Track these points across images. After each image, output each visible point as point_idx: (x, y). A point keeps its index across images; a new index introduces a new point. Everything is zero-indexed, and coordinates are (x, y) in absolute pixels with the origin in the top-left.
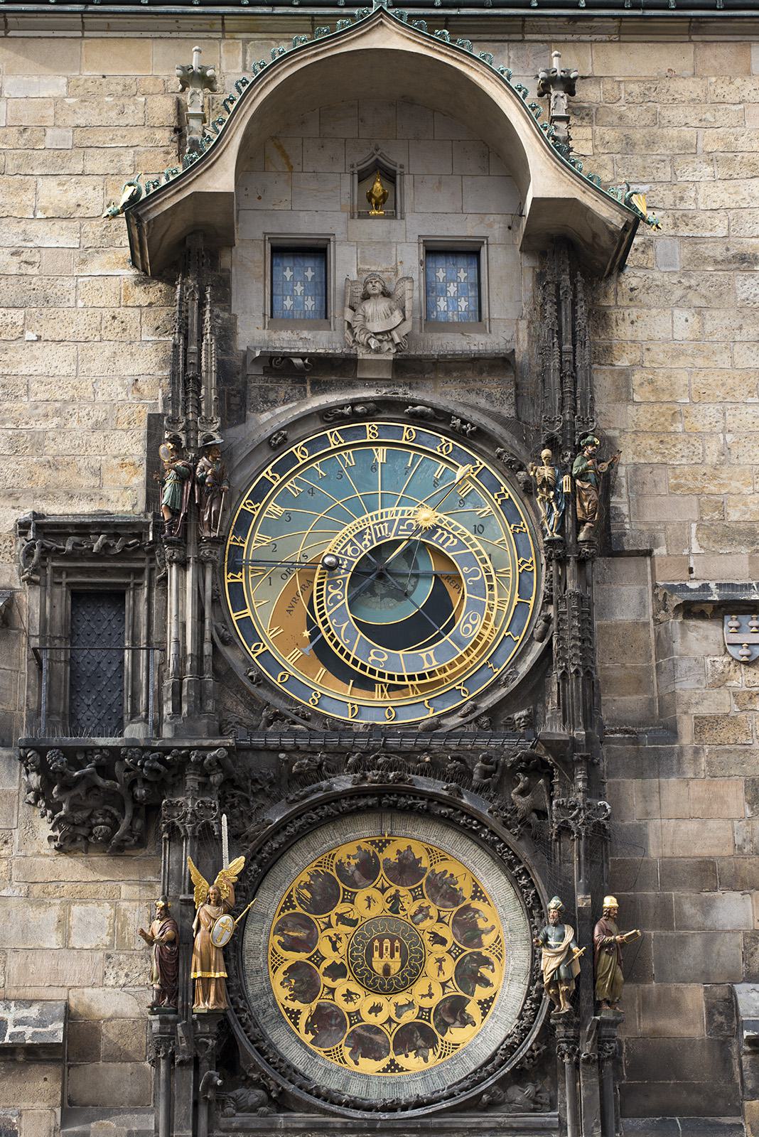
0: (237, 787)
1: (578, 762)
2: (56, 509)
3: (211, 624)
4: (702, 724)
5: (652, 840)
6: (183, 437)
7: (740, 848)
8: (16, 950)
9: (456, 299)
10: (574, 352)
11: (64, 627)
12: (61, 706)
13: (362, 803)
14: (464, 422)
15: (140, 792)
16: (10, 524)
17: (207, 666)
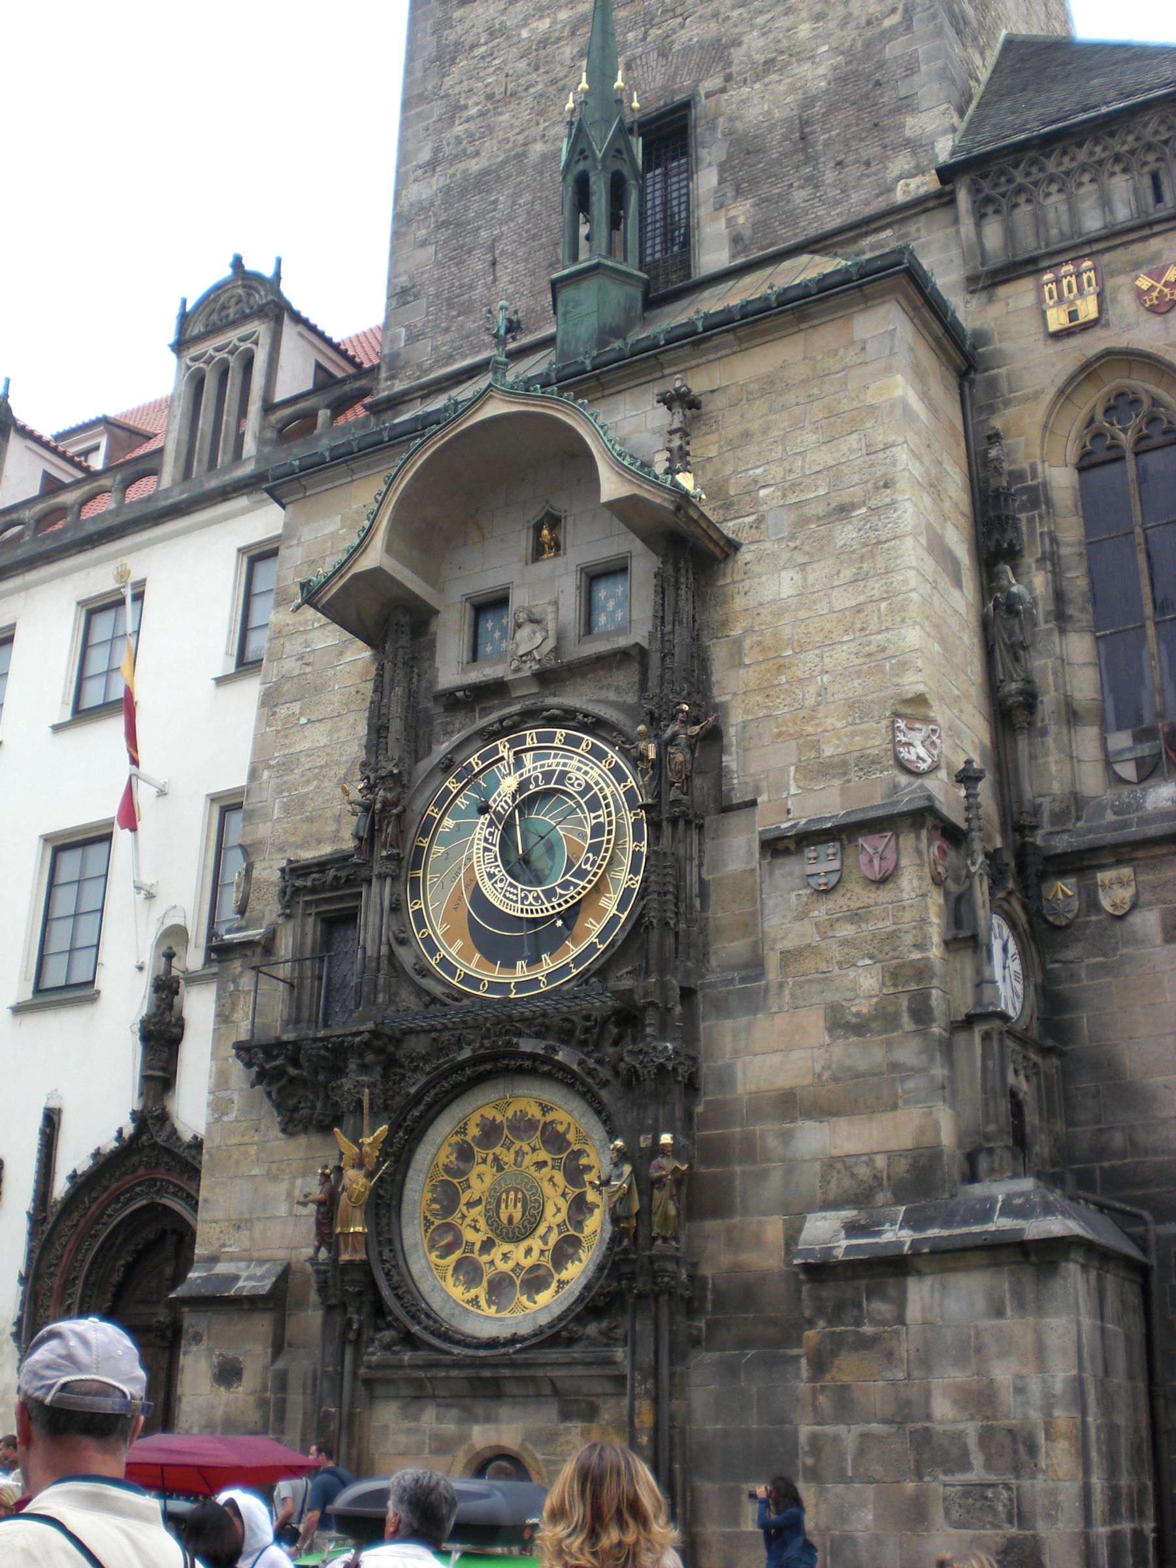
0: (402, 1066)
1: (643, 1009)
2: (308, 855)
3: (388, 928)
4: (788, 957)
5: (740, 1075)
6: (372, 776)
7: (819, 1076)
8: (259, 1219)
9: (613, 612)
10: (673, 632)
11: (313, 949)
12: (305, 1014)
13: (482, 1068)
14: (586, 716)
15: (321, 1077)
16: (279, 874)
17: (384, 963)
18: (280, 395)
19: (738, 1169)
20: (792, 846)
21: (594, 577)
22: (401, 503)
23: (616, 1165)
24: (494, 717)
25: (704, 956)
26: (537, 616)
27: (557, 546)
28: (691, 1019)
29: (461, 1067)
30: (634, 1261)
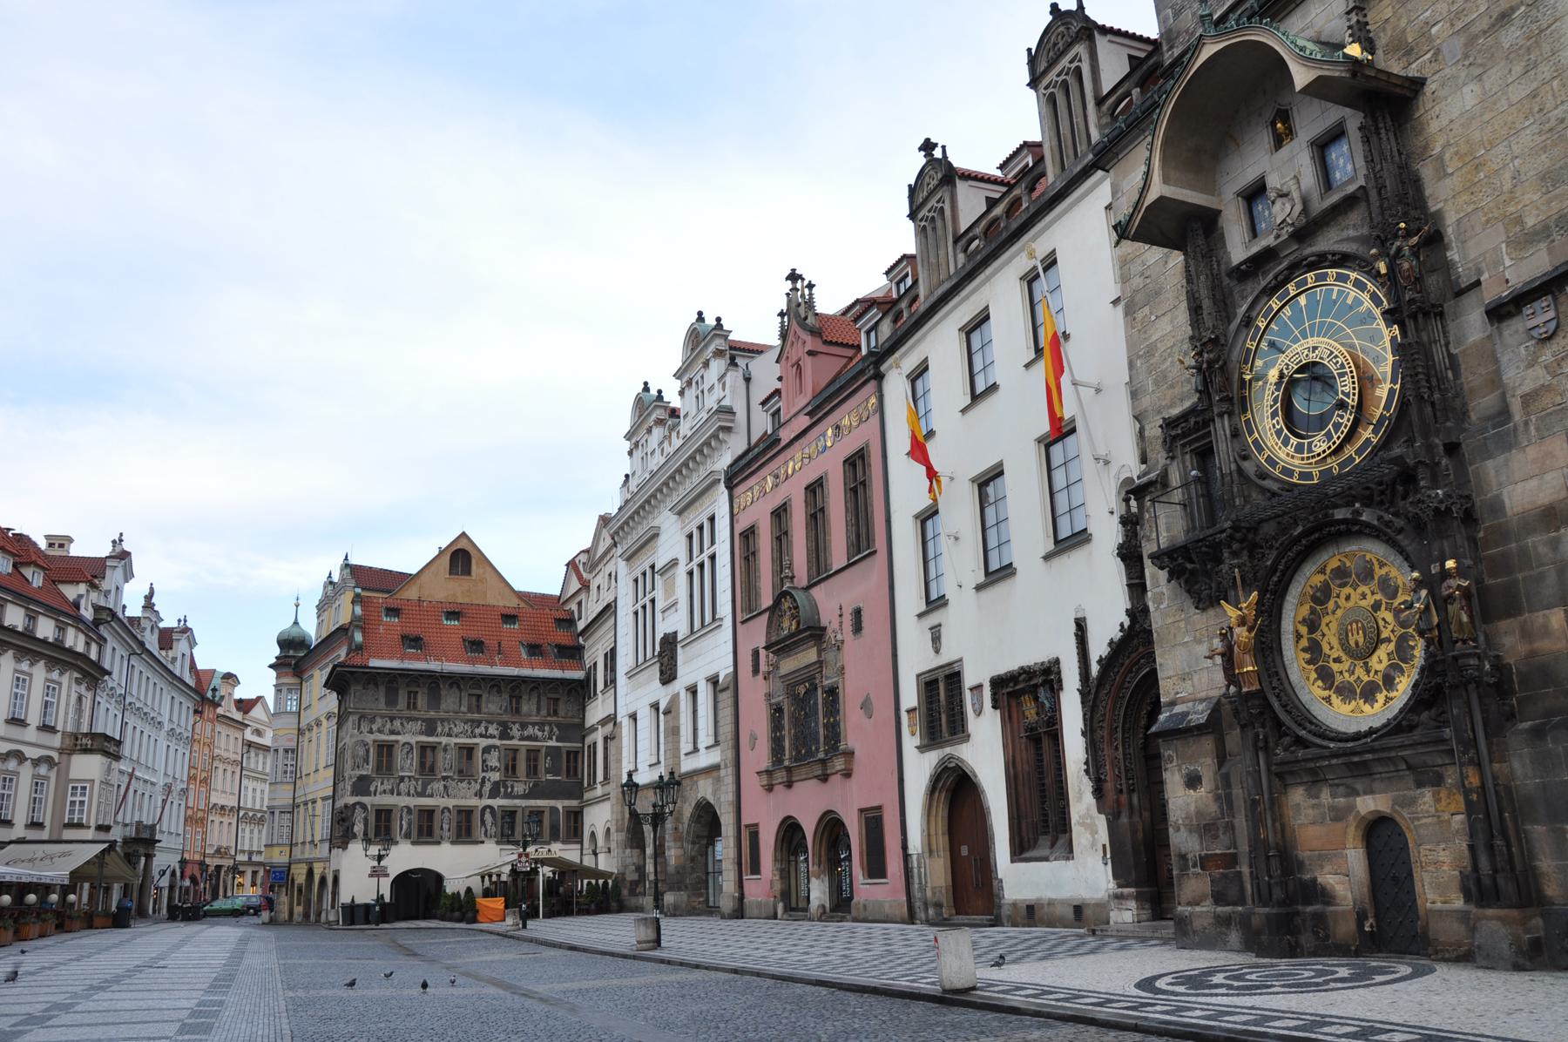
1: (1415, 468)
2: (1176, 411)
4: (1528, 399)
5: (1507, 501)
18: (1106, 89)
19: (1520, 576)
20: (1512, 308)
21: (1321, 147)
22: (1165, 143)
23: (1415, 591)
24: (1271, 276)
25: (1464, 414)
26: (1285, 190)
27: (1290, 133)
28: (1461, 467)
29: (1297, 540)
30: (1443, 661)
